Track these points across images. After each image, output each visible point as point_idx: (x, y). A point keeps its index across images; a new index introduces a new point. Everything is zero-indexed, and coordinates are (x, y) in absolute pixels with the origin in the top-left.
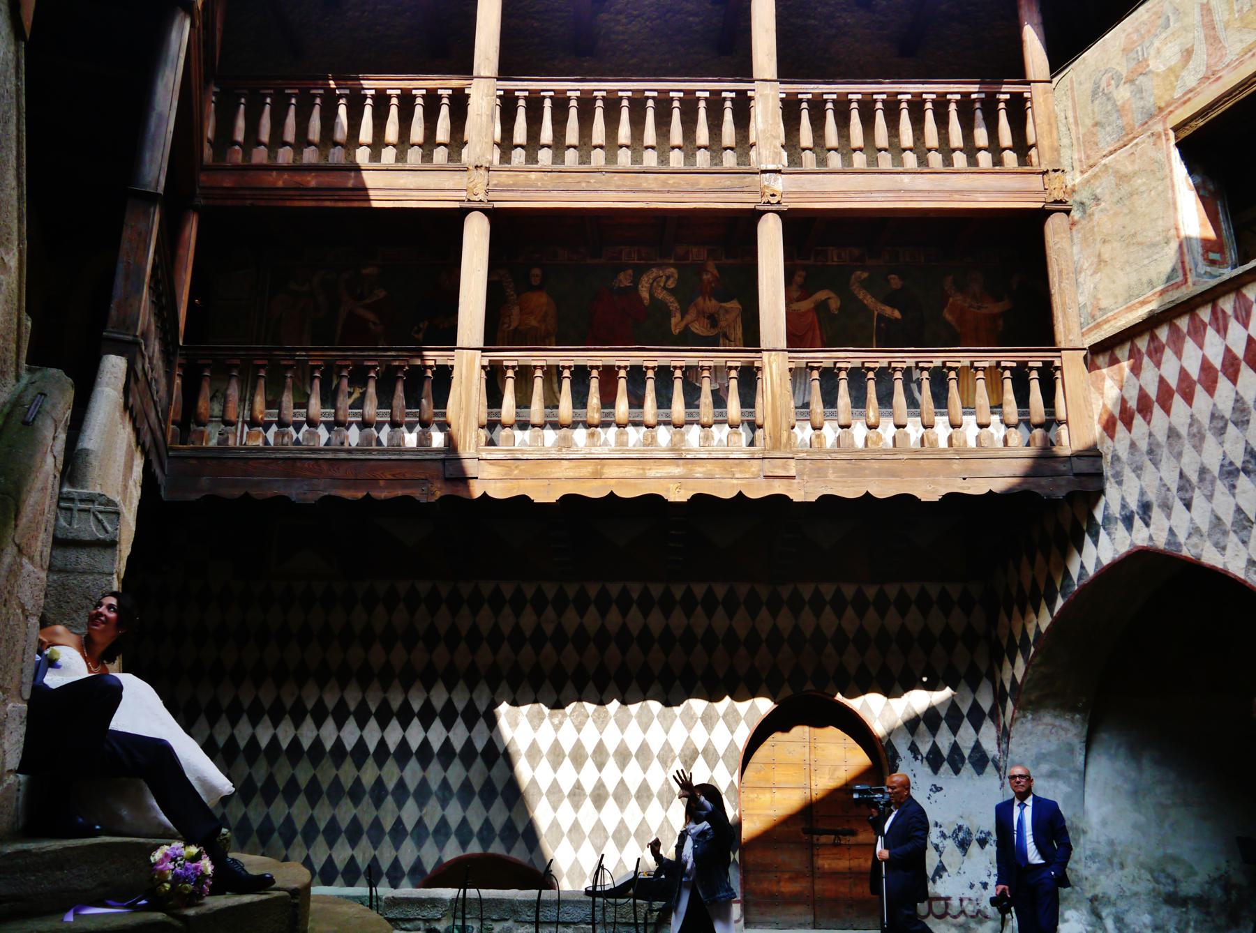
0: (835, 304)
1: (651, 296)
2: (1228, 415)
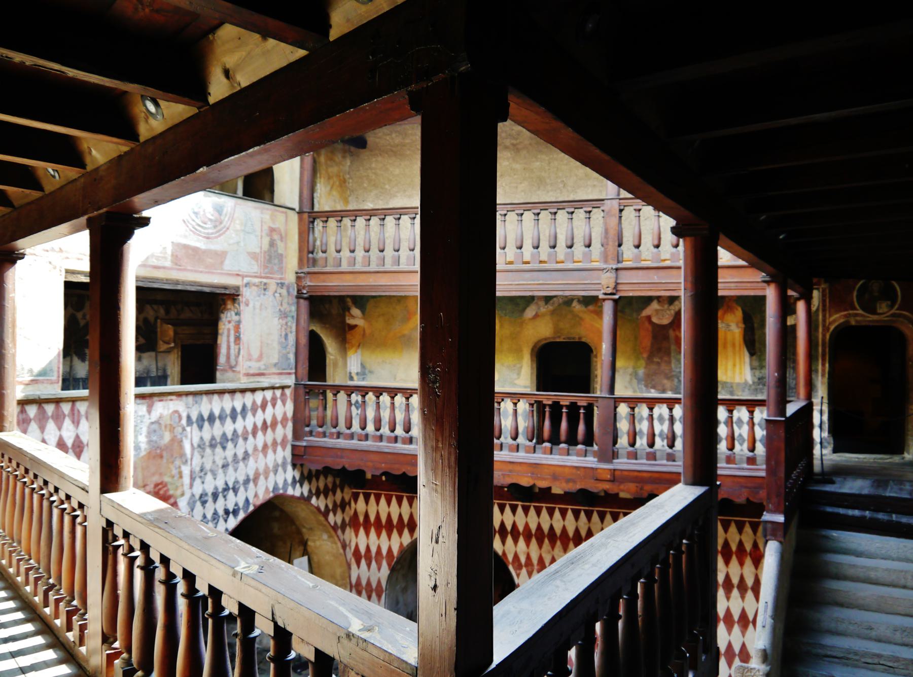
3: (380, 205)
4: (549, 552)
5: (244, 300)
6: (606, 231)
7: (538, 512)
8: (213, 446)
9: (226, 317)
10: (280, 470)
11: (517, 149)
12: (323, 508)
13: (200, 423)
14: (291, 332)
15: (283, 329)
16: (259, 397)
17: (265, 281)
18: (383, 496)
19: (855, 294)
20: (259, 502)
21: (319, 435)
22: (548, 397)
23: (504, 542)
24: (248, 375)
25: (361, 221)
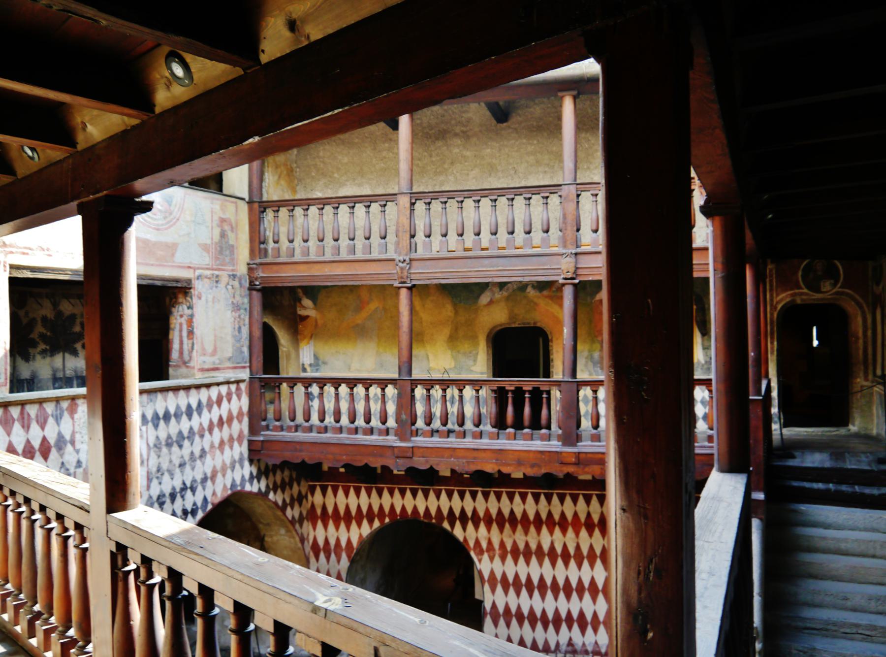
3: (329, 193)
4: (510, 536)
5: (196, 293)
6: (565, 216)
7: (499, 497)
8: (169, 445)
9: (178, 312)
10: (237, 466)
11: (468, 136)
12: (280, 503)
13: (156, 422)
14: (244, 325)
15: (236, 322)
16: (214, 392)
17: (216, 273)
18: (340, 487)
19: (800, 273)
20: (217, 500)
21: (276, 429)
22: (510, 383)
23: (464, 529)
24: (202, 370)
25: (313, 210)
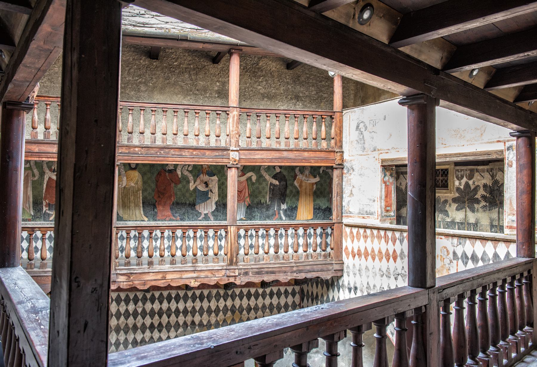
0: (254, 178)
1: (182, 174)
2: (385, 272)
13: (465, 260)
